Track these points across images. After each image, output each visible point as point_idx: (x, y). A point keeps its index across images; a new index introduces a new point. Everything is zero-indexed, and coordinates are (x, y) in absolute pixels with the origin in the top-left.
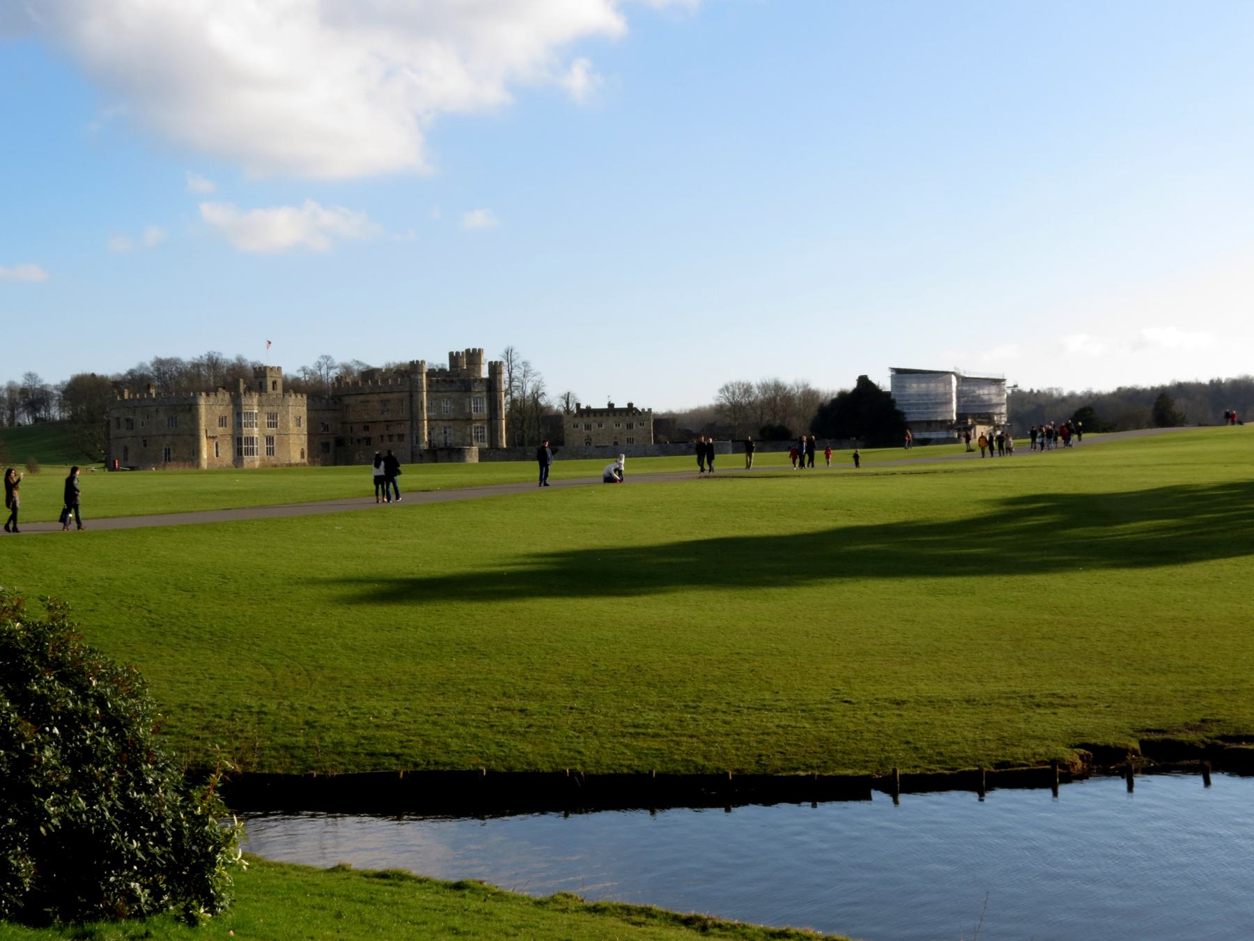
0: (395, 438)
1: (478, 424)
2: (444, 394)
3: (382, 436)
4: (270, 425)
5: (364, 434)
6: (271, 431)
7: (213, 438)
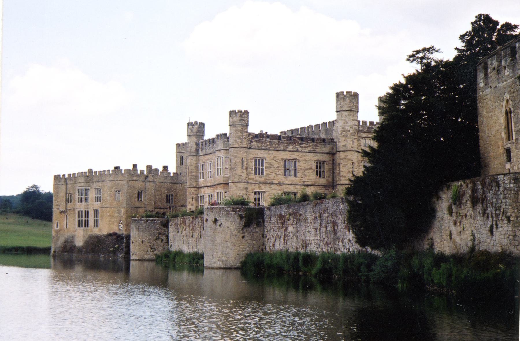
6: (97, 205)
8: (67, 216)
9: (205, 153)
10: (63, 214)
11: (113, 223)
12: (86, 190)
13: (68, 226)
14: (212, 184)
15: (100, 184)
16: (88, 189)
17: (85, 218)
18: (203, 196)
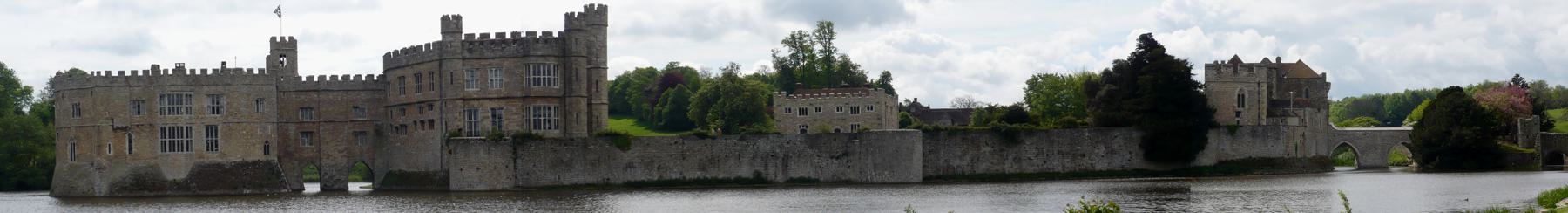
0: (427, 125)
1: (540, 103)
2: (491, 61)
3: (415, 122)
4: (215, 110)
5: (401, 120)
6: (212, 119)
7: (122, 129)
8: (130, 136)
9: (478, 56)
10: (120, 133)
11: (254, 145)
12: (186, 95)
13: (134, 150)
14: (502, 96)
15: (220, 89)
16: (190, 95)
17: (187, 137)
18: (476, 111)
